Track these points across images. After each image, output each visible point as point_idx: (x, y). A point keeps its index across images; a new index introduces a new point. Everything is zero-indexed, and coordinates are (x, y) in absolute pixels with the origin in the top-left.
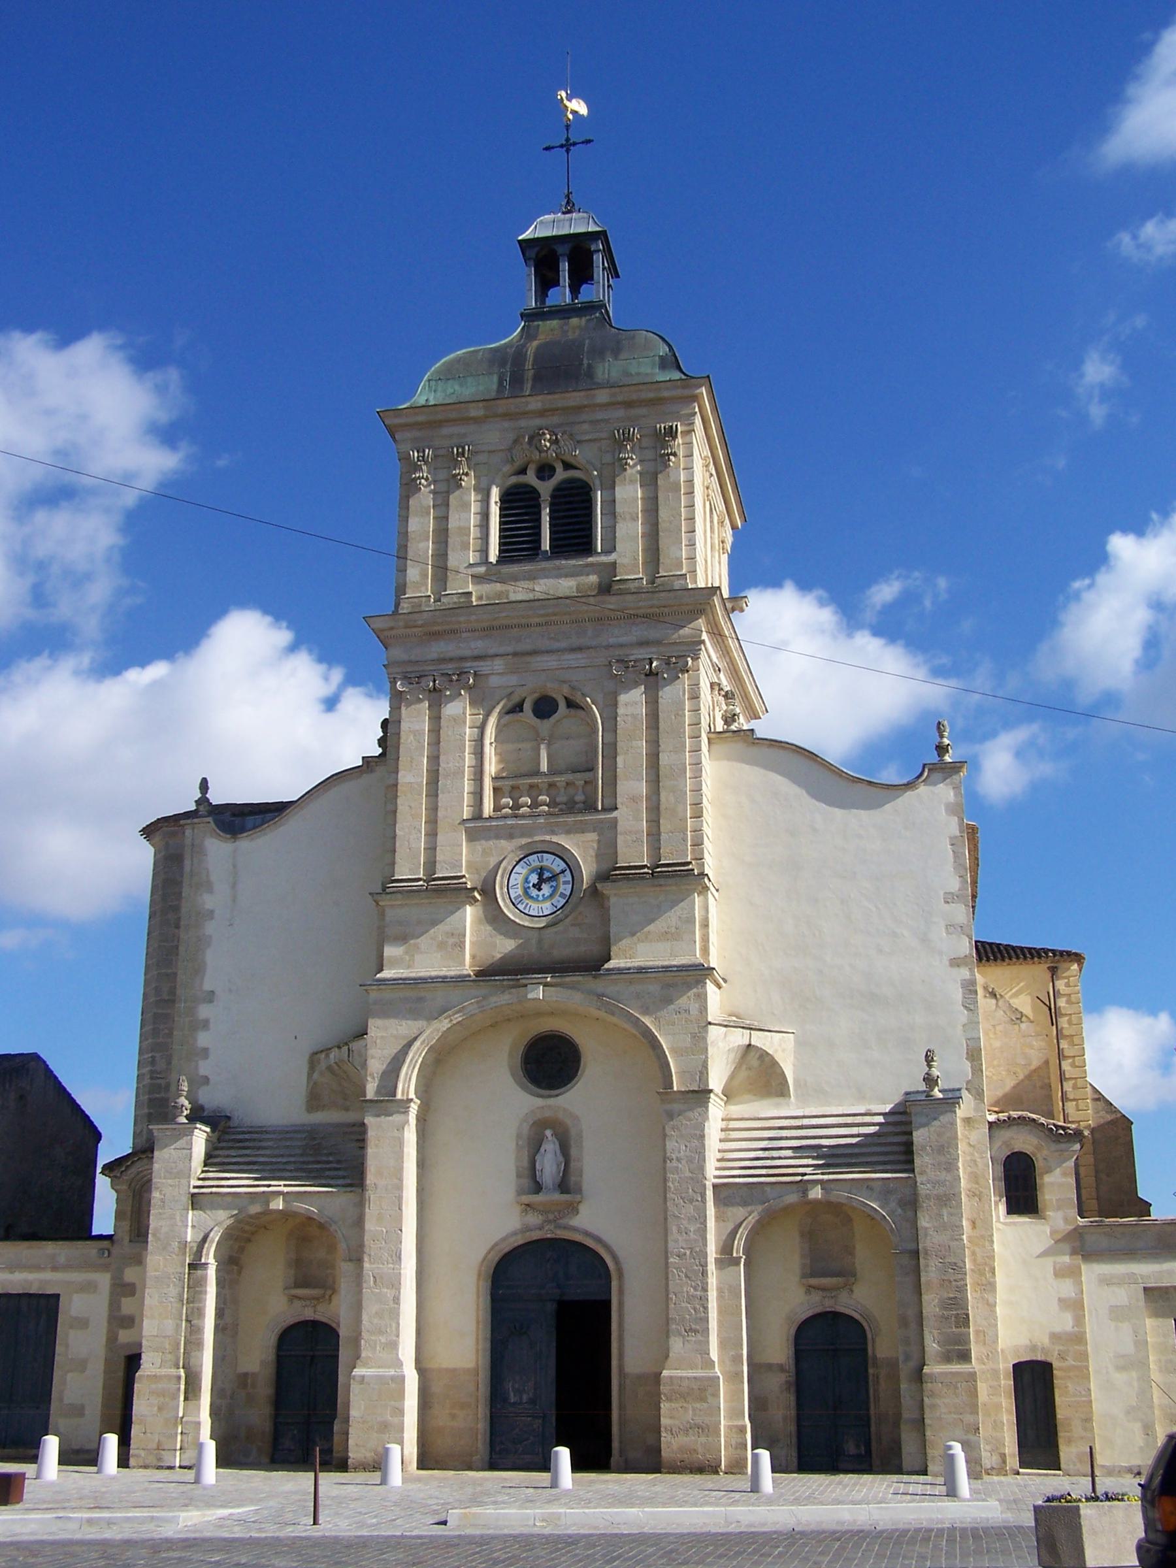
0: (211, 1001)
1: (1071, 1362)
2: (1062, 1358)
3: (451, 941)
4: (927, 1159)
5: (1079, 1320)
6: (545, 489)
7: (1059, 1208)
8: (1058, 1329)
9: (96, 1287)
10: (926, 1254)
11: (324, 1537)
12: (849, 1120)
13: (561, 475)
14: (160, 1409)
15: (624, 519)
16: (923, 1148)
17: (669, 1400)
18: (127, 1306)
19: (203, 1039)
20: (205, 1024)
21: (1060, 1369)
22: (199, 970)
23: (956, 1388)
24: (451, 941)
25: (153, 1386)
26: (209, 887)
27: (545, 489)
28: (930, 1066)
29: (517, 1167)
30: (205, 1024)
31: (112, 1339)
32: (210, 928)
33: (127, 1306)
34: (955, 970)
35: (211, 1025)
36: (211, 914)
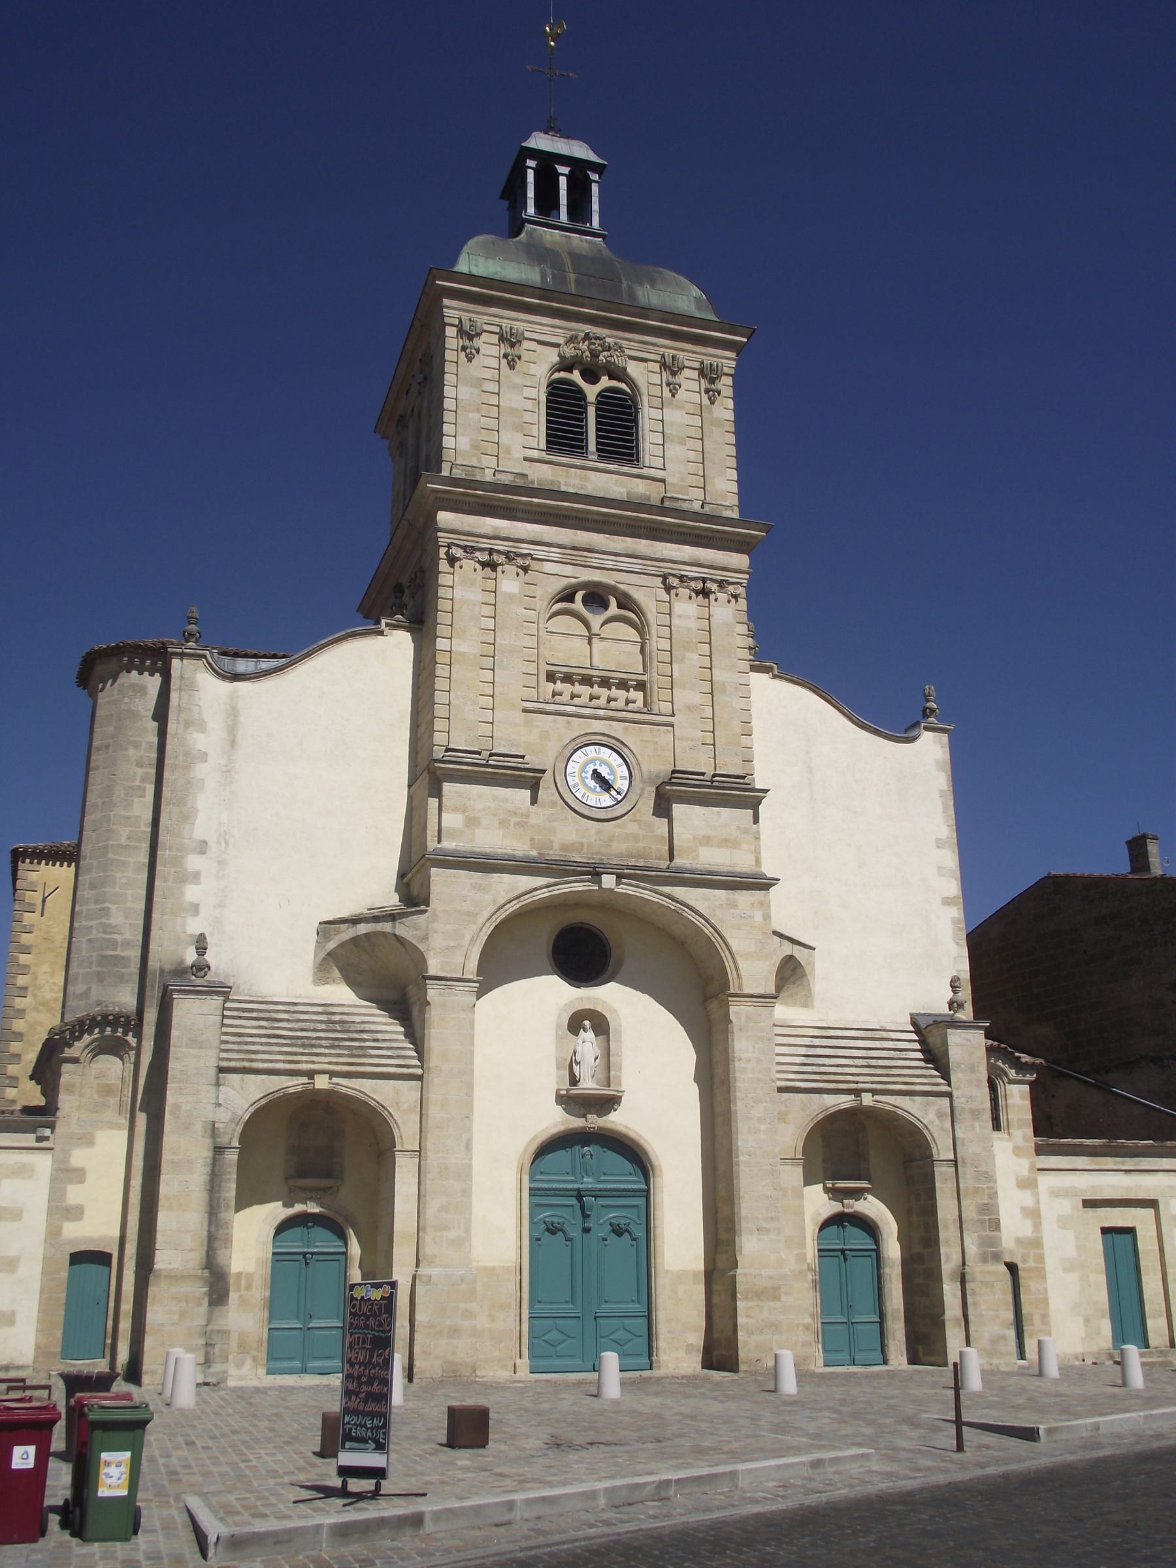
0: (203, 852)
1: (1031, 1264)
2: (1025, 1261)
3: (514, 820)
4: (960, 1075)
5: (1037, 1227)
6: (591, 392)
7: (1019, 1127)
8: (1021, 1234)
9: (33, 1171)
10: (964, 1162)
11: (1006, 1476)
12: (869, 1034)
13: (605, 382)
14: (182, 1315)
15: (672, 441)
16: (958, 1065)
17: (746, 1299)
18: (74, 1194)
19: (192, 893)
20: (196, 877)
21: (1024, 1270)
22: (187, 818)
23: (993, 1286)
24: (514, 820)
25: (173, 1290)
26: (202, 727)
27: (591, 392)
28: (955, 992)
29: (557, 1059)
30: (196, 877)
31: (53, 1234)
32: (201, 770)
33: (74, 1194)
34: (947, 908)
35: (202, 879)
36: (204, 757)
